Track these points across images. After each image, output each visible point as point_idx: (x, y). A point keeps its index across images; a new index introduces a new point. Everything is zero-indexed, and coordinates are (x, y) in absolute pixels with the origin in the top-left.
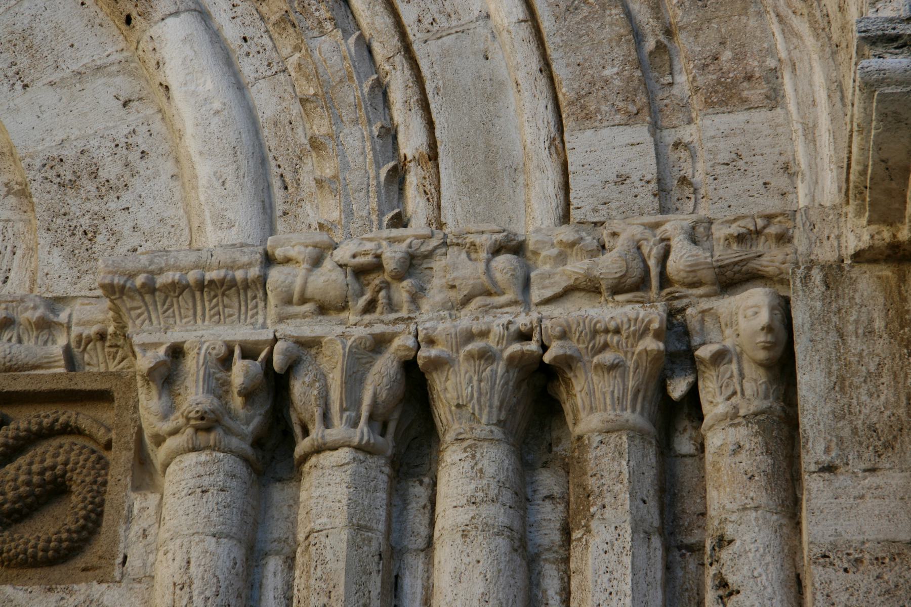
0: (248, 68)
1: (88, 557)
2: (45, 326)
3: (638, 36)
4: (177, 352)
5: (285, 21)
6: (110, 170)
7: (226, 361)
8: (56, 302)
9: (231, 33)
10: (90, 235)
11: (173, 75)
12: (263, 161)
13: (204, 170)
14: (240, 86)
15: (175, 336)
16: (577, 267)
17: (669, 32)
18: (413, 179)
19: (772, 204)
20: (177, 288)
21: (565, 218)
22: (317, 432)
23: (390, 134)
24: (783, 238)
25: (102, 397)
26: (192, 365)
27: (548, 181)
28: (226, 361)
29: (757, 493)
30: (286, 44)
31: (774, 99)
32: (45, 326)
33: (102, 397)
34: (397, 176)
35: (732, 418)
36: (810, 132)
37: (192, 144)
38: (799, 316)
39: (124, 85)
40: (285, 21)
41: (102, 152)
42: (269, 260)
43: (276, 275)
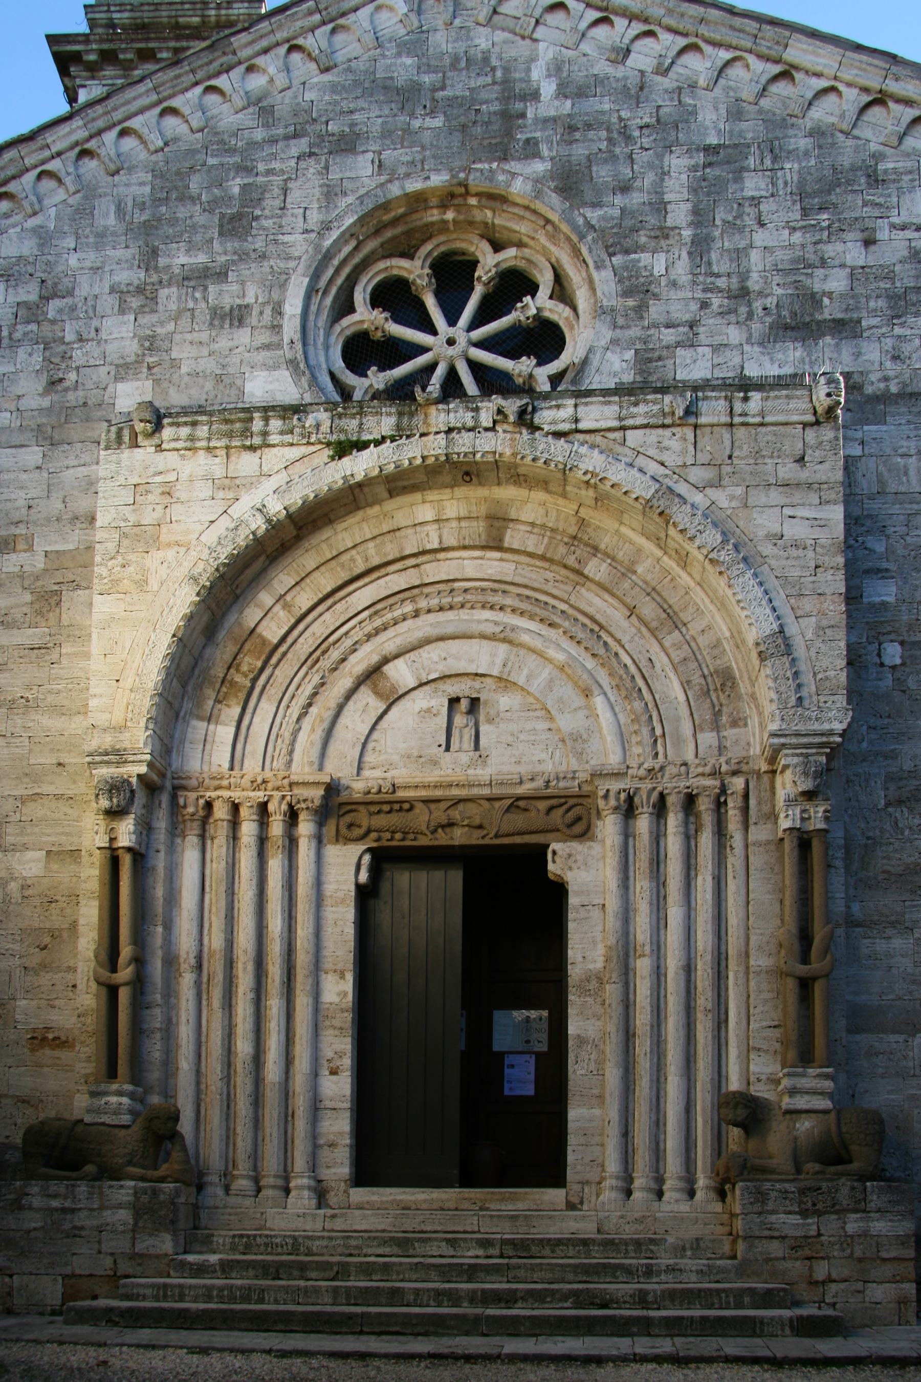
0: (617, 709)
1: (590, 834)
2: (573, 778)
3: (714, 706)
4: (608, 791)
5: (626, 697)
6: (585, 737)
7: (619, 793)
8: (575, 772)
9: (612, 699)
10: (581, 754)
11: (599, 712)
12: (622, 735)
13: (609, 739)
14: (615, 714)
15: (607, 787)
16: (700, 770)
17: (721, 705)
18: (659, 742)
19: (744, 754)
20: (607, 775)
21: (697, 756)
22: (640, 810)
23: (653, 729)
24: (747, 763)
25: (588, 796)
26: (612, 794)
27: (692, 746)
28: (619, 793)
29: (739, 826)
30: (627, 703)
31: (746, 725)
32: (573, 778)
33: (588, 796)
34: (656, 741)
35: (734, 808)
36: (754, 734)
37: (605, 731)
38: (751, 786)
39: (586, 712)
40: (626, 697)
41: (583, 732)
42: (628, 767)
43: (630, 771)
